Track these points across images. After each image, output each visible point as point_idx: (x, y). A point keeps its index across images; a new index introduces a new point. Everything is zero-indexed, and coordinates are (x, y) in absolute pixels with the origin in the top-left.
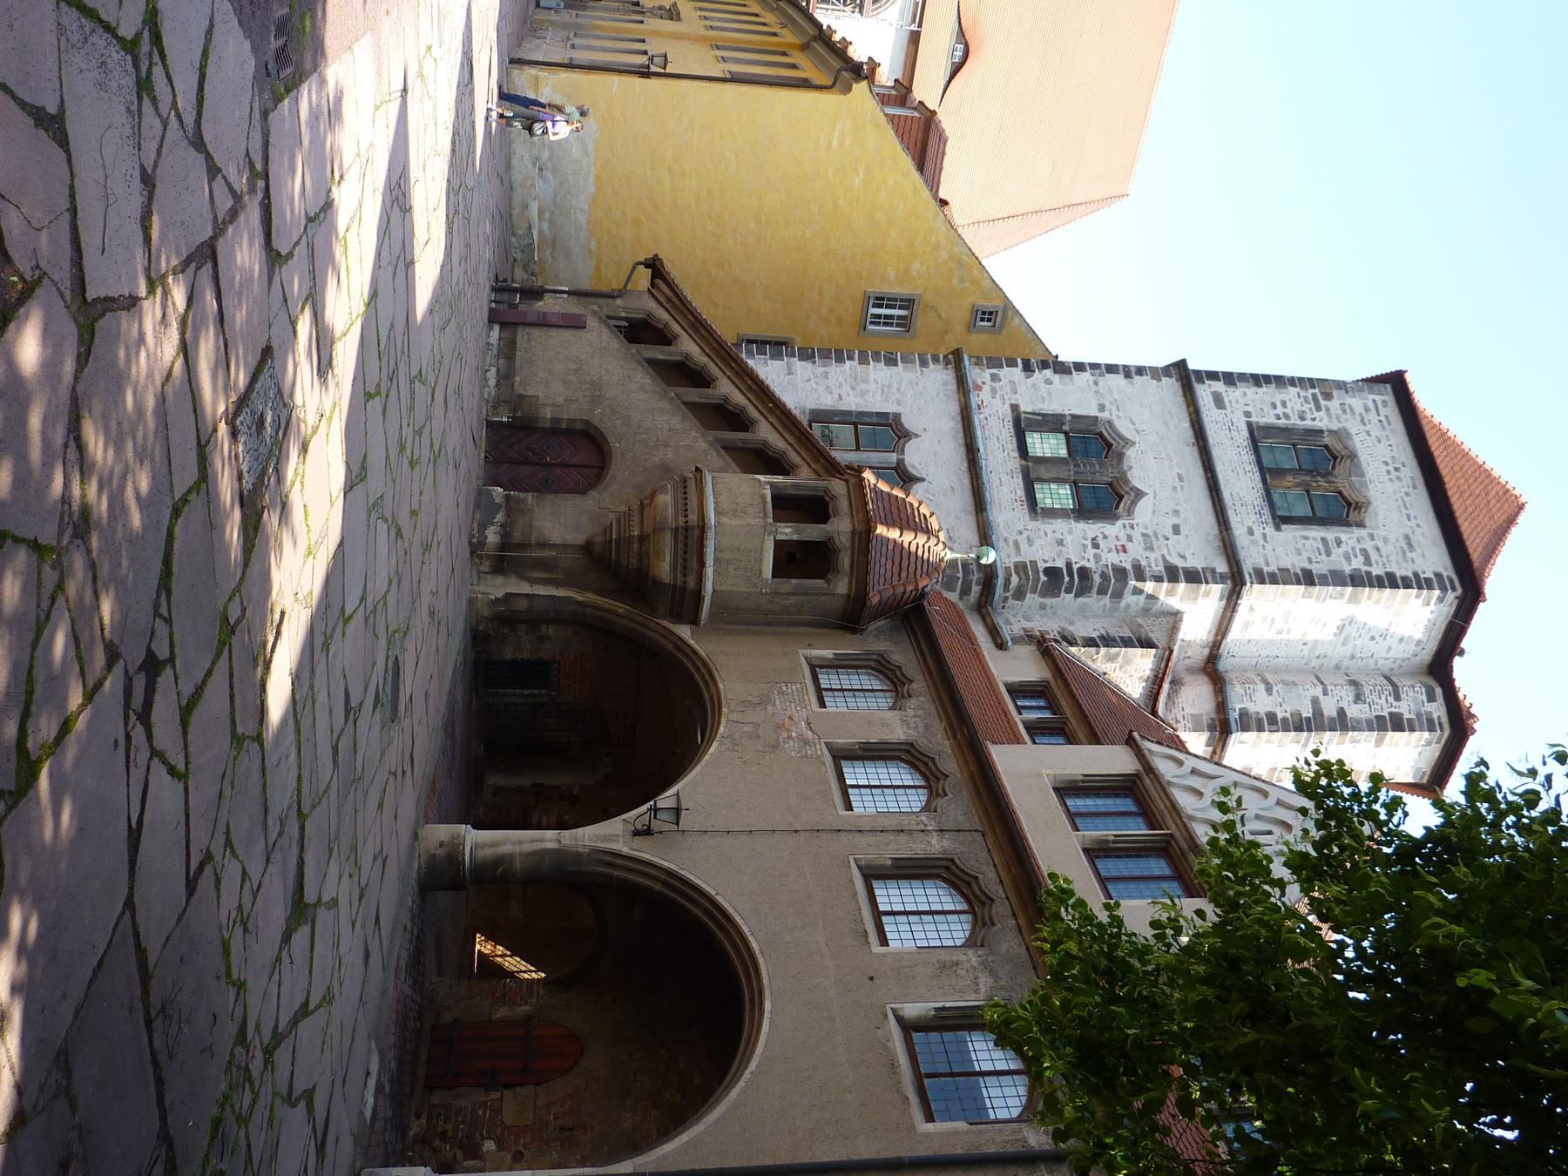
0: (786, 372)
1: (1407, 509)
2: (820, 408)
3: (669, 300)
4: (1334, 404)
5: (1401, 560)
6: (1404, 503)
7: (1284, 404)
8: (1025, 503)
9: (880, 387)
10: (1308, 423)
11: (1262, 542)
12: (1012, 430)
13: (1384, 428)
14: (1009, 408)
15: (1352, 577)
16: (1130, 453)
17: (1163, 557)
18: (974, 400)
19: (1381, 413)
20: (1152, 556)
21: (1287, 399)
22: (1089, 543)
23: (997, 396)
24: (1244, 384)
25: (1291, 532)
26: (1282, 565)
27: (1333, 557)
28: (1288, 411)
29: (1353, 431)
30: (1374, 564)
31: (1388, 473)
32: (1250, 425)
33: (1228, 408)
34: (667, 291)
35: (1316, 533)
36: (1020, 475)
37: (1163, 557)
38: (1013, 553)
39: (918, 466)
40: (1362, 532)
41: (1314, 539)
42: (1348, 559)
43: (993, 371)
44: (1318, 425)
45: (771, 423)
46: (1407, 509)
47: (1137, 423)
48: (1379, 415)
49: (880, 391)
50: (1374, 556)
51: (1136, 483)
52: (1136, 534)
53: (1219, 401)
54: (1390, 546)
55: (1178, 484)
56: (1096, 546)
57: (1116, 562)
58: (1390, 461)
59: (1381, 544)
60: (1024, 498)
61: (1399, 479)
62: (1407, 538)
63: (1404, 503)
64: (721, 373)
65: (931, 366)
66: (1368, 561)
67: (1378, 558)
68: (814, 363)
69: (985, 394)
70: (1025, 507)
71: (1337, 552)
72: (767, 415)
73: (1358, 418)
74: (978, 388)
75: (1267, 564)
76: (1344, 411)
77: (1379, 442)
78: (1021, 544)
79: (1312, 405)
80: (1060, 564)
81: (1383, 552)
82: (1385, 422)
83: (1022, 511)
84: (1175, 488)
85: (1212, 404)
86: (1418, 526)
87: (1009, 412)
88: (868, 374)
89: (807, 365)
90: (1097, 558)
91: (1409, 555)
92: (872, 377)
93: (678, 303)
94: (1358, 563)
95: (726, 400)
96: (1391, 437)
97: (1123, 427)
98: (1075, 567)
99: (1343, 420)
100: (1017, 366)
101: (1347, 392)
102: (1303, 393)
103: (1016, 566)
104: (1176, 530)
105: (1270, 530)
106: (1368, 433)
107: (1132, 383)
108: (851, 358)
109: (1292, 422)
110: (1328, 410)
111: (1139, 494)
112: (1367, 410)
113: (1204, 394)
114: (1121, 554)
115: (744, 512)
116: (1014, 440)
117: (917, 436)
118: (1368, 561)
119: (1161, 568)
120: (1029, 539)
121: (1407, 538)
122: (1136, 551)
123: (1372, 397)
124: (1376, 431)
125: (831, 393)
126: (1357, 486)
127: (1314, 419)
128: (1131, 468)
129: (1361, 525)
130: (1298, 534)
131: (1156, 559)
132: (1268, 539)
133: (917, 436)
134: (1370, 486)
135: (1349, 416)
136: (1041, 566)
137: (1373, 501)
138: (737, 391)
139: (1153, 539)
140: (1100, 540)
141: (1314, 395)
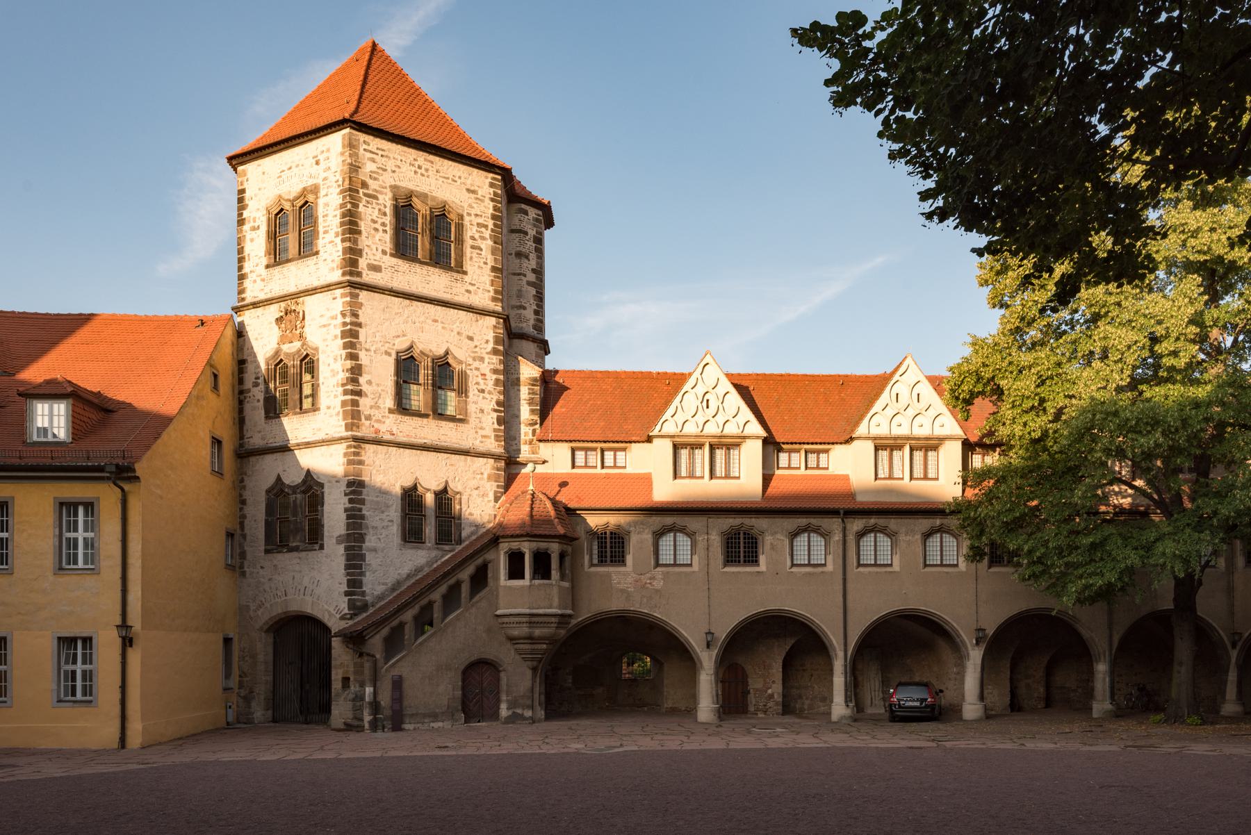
0: (374, 553)
1: (448, 178)
2: (400, 535)
4: (373, 185)
5: (482, 204)
6: (444, 178)
7: (374, 222)
10: (388, 211)
11: (475, 288)
13: (387, 156)
14: (391, 415)
15: (495, 243)
16: (420, 347)
17: (487, 353)
18: (387, 437)
19: (376, 151)
20: (487, 360)
21: (370, 218)
22: (482, 395)
23: (383, 420)
24: (359, 243)
25: (468, 266)
26: (488, 283)
27: (483, 246)
28: (380, 221)
29: (393, 183)
30: (486, 223)
31: (422, 175)
32: (392, 255)
33: (381, 264)
35: (468, 251)
37: (487, 353)
38: (488, 441)
39: (437, 483)
40: (467, 219)
41: (472, 253)
42: (483, 238)
43: (363, 418)
44: (389, 203)
46: (448, 178)
47: (397, 334)
48: (377, 154)
50: (481, 220)
51: (441, 352)
52: (476, 364)
53: (376, 268)
54: (475, 205)
55: (440, 325)
56: (483, 391)
57: (492, 382)
58: (413, 169)
59: (473, 212)
61: (427, 170)
62: (468, 190)
63: (444, 178)
66: (486, 227)
67: (483, 218)
68: (365, 534)
69: (383, 428)
71: (479, 243)
73: (380, 171)
74: (377, 431)
75: (489, 291)
76: (375, 179)
77: (399, 167)
79: (374, 201)
80: (495, 415)
81: (479, 213)
82: (383, 153)
83: (462, 427)
84: (443, 328)
85: (378, 274)
86: (460, 178)
88: (372, 501)
89: (367, 538)
90: (490, 393)
91: (479, 196)
92: (375, 499)
94: (487, 233)
96: (396, 156)
97: (402, 344)
98: (496, 407)
99: (384, 185)
100: (357, 400)
101: (360, 168)
102: (364, 202)
103: (497, 441)
104: (471, 339)
105: (467, 278)
106: (394, 172)
107: (366, 325)
108: (360, 510)
109: (387, 222)
110: (376, 190)
111: (447, 353)
112: (373, 161)
113: (370, 276)
114: (487, 377)
116: (414, 418)
117: (416, 479)
118: (486, 227)
119: (494, 357)
120: (481, 428)
121: (468, 190)
122: (486, 368)
123: (361, 151)
124: (390, 165)
125: (387, 526)
126: (434, 204)
127: (385, 207)
128: (431, 351)
129: (461, 217)
130: (469, 262)
131: (489, 358)
132: (473, 282)
133: (416, 479)
134: (434, 195)
135: (381, 178)
136: (496, 426)
137: (445, 199)
139: (476, 355)
140: (480, 387)
141: (365, 195)
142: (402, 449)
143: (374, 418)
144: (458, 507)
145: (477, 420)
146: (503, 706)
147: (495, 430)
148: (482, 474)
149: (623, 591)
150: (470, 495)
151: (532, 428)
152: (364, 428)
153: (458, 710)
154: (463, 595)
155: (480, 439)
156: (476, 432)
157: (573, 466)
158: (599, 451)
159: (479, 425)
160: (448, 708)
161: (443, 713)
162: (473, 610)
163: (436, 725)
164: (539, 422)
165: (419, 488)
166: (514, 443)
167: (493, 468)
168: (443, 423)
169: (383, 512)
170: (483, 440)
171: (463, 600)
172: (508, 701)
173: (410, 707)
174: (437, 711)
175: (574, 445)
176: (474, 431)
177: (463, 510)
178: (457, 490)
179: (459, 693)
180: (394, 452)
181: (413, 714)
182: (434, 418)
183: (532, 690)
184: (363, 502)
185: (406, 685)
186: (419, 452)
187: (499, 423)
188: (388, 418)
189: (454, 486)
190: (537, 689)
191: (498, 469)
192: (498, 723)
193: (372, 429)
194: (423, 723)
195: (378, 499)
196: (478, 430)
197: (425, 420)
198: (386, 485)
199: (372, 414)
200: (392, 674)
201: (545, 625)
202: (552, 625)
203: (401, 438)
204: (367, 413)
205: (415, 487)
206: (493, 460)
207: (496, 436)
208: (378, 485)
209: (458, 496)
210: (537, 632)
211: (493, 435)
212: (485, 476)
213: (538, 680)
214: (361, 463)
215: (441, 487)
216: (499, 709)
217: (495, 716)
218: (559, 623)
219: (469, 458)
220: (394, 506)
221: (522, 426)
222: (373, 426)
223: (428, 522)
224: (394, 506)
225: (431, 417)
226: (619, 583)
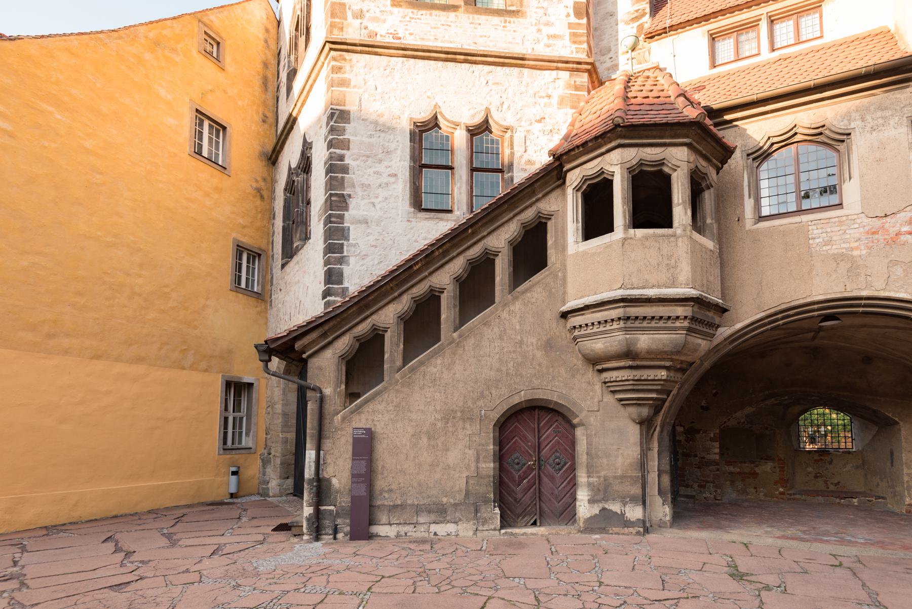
0: (364, 226)
3: (324, 335)
8: (508, 19)
9: (378, 134)
12: (424, 12)
23: (383, 18)
34: (314, 335)
36: (476, 16)
38: (558, 43)
39: (472, 112)
43: (349, 15)
45: (489, 234)
49: (383, 135)
60: (502, 19)
64: (424, 282)
65: (347, 76)
70: (512, 20)
72: (479, 236)
78: (552, 33)
87: (401, 10)
92: (367, 140)
93: (331, 324)
95: (457, 279)
103: (575, 42)
115: (669, 258)
117: (436, 106)
120: (547, 24)
133: (436, 106)
136: (573, 19)
138: (447, 267)
142: (412, 61)
143: (367, 15)
144: (507, 152)
145: (541, 12)
146: (583, 495)
147: (570, 26)
148: (549, 97)
149: (838, 258)
150: (528, 131)
151: (637, 23)
152: (350, 30)
153: (486, 501)
154: (498, 279)
155: (545, 41)
156: (539, 30)
157: (714, 65)
158: (764, 25)
159: (544, 19)
160: (467, 494)
161: (455, 505)
162: (517, 306)
163: (442, 529)
164: (648, 10)
165: (442, 122)
166: (607, 58)
167: (569, 86)
168: (483, 18)
169: (380, 161)
170: (551, 42)
171: (498, 289)
172: (589, 484)
173: (391, 491)
174: (445, 500)
175: (714, 25)
176: (534, 29)
177: (517, 155)
178: (505, 124)
179: (489, 467)
180: (400, 65)
181: (395, 507)
182: (466, 11)
183: (642, 465)
184: (345, 145)
185: (381, 449)
186: (440, 64)
187: (577, 14)
188: (391, 13)
189: (498, 119)
190: (654, 464)
191: (577, 88)
192: (572, 528)
193: (363, 31)
194: (415, 525)
195: (371, 140)
196: (542, 27)
197: (452, 15)
198: (385, 117)
199: (365, 9)
200: (354, 425)
201: (661, 324)
202: (678, 324)
203: (410, 41)
204: (356, 8)
205: (433, 124)
206: (568, 73)
207: (574, 35)
208: (373, 117)
209: (508, 135)
210: (644, 341)
211: (567, 33)
212: (555, 100)
213: (655, 445)
214: (344, 83)
215: (478, 120)
216: (575, 499)
217: (567, 513)
218: (693, 319)
219: (526, 71)
220: (399, 152)
221: (621, 27)
222: (366, 28)
223: (457, 176)
224: (399, 152)
225: (461, 10)
226: (829, 242)
